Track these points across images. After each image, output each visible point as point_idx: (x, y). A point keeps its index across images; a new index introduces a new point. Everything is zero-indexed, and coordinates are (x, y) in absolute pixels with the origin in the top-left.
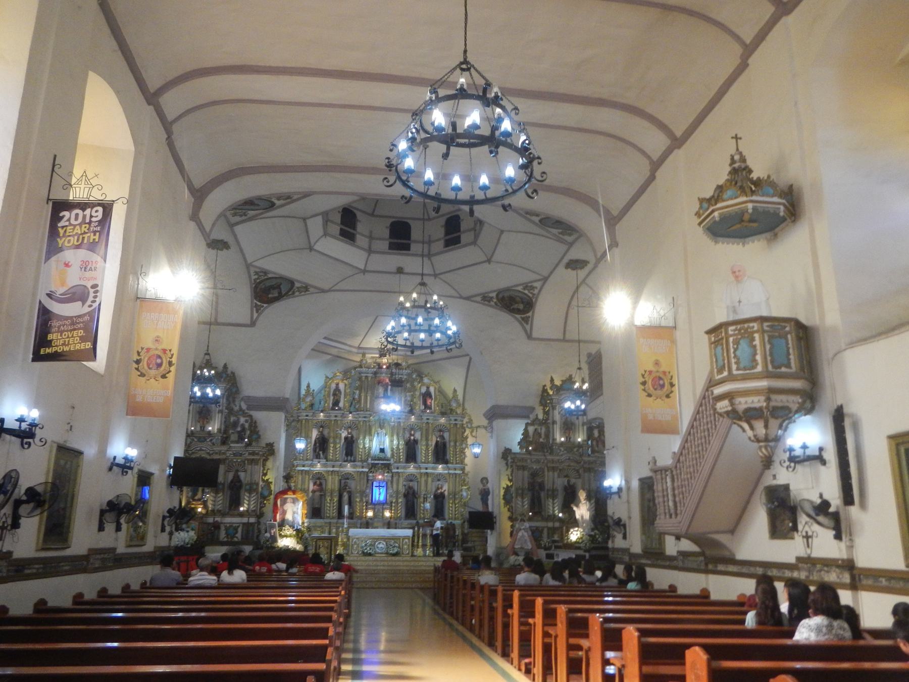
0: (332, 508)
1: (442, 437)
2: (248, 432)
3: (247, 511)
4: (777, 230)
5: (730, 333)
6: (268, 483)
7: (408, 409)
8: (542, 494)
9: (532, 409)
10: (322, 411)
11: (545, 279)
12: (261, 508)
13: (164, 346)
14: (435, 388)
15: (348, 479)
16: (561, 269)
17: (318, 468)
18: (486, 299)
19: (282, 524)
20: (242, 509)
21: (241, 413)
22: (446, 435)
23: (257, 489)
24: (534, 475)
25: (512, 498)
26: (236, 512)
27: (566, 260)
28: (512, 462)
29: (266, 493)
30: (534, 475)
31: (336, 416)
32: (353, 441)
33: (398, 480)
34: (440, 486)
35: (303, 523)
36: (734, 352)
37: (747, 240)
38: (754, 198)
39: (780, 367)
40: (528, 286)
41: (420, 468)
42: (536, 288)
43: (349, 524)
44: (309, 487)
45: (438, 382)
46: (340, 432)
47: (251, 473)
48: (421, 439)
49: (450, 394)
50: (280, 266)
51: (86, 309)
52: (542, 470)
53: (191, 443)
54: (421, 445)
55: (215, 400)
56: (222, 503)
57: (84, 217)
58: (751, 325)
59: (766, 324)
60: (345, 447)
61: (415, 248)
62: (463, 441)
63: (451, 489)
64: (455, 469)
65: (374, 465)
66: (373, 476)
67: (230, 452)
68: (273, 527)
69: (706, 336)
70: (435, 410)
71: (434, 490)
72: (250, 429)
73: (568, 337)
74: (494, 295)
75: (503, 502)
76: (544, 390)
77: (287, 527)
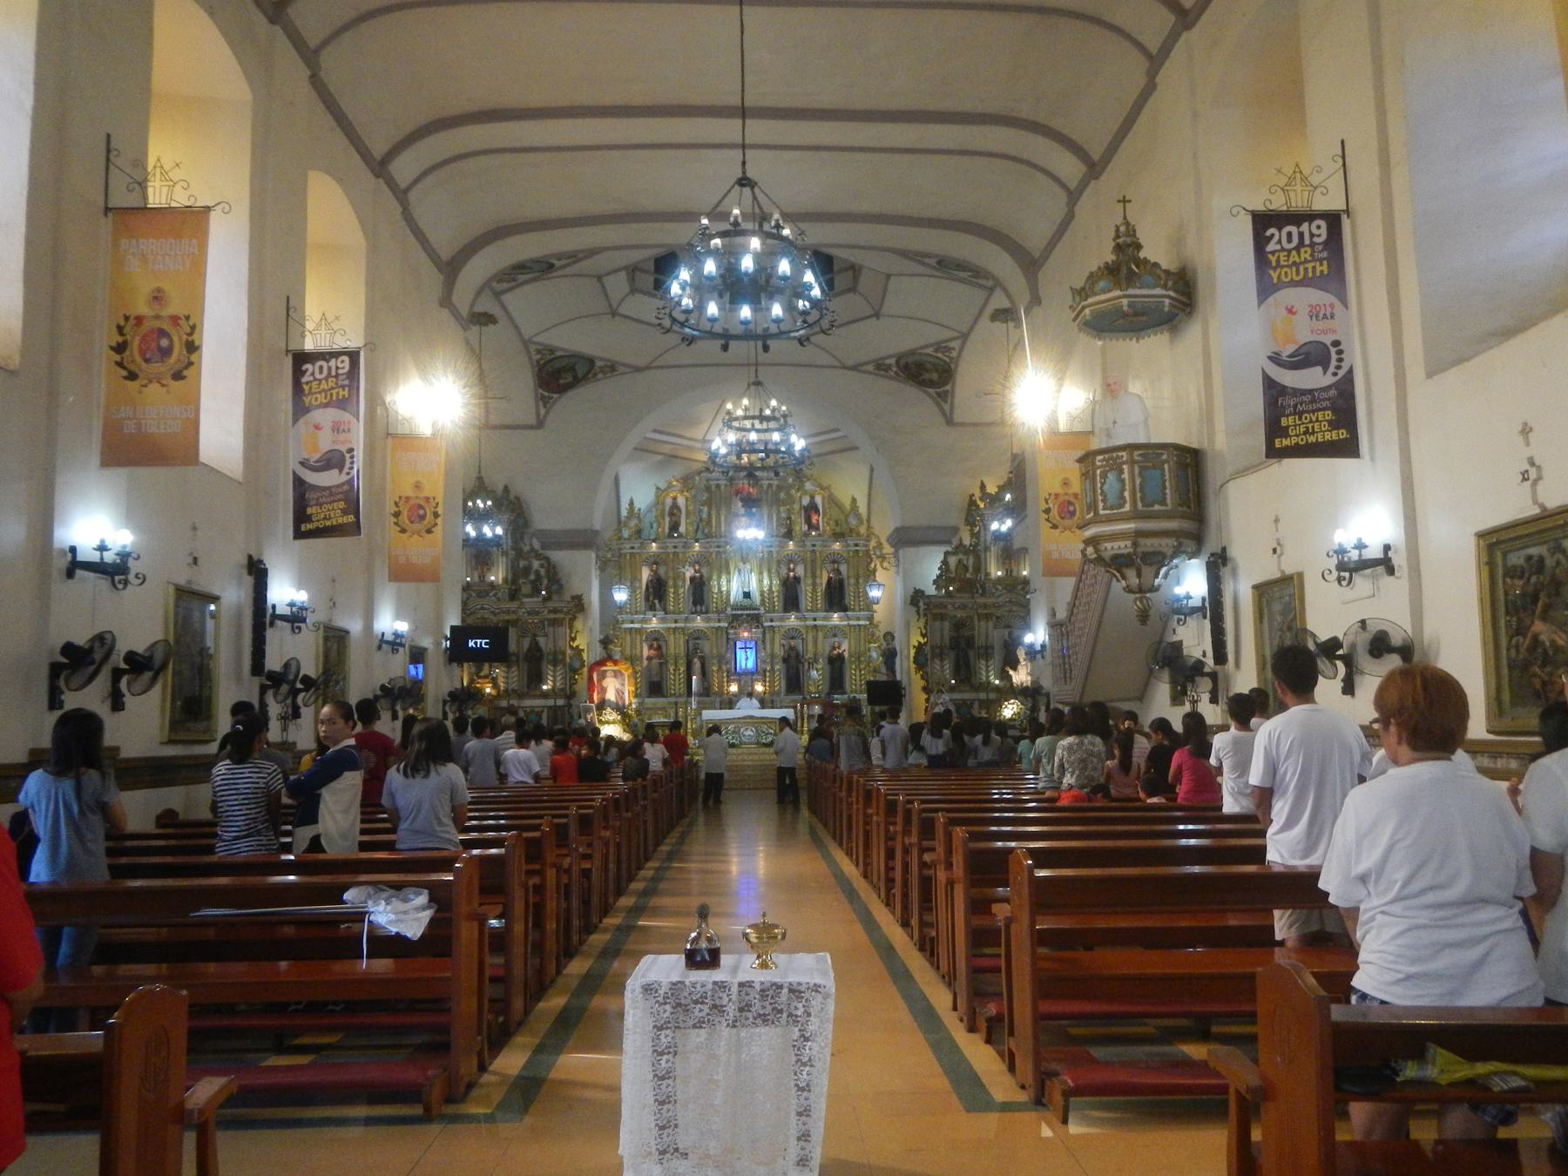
0: (677, 682)
1: (838, 572)
2: (545, 582)
3: (553, 689)
4: (1175, 322)
5: (1098, 463)
6: (578, 651)
7: (783, 530)
8: (971, 653)
9: (955, 530)
10: (654, 541)
11: (964, 337)
12: (571, 685)
13: (426, 493)
14: (823, 498)
15: (698, 638)
17: (654, 623)
18: (880, 367)
19: (602, 705)
20: (545, 687)
21: (533, 554)
22: (843, 568)
23: (564, 660)
24: (959, 625)
25: (927, 660)
26: (538, 693)
28: (925, 609)
29: (577, 665)
30: (959, 625)
31: (675, 547)
32: (704, 583)
33: (773, 639)
34: (836, 645)
35: (630, 704)
36: (1101, 488)
37: (1143, 333)
38: (1131, 291)
39: (1153, 506)
40: (940, 346)
41: (805, 619)
42: (953, 349)
43: (698, 703)
44: (642, 651)
45: (828, 488)
46: (683, 570)
47: (554, 638)
48: (805, 576)
49: (847, 504)
50: (571, 340)
51: (344, 478)
52: (971, 618)
53: (468, 599)
54: (806, 585)
55: (496, 541)
56: (518, 681)
57: (329, 368)
58: (1120, 454)
59: (1136, 453)
60: (691, 592)
62: (869, 576)
63: (853, 649)
64: (858, 619)
65: (735, 618)
66: (735, 633)
67: (524, 610)
68: (588, 710)
69: (1077, 465)
70: (824, 531)
71: (827, 651)
72: (548, 576)
74: (892, 361)
75: (913, 666)
76: (972, 503)
77: (609, 709)
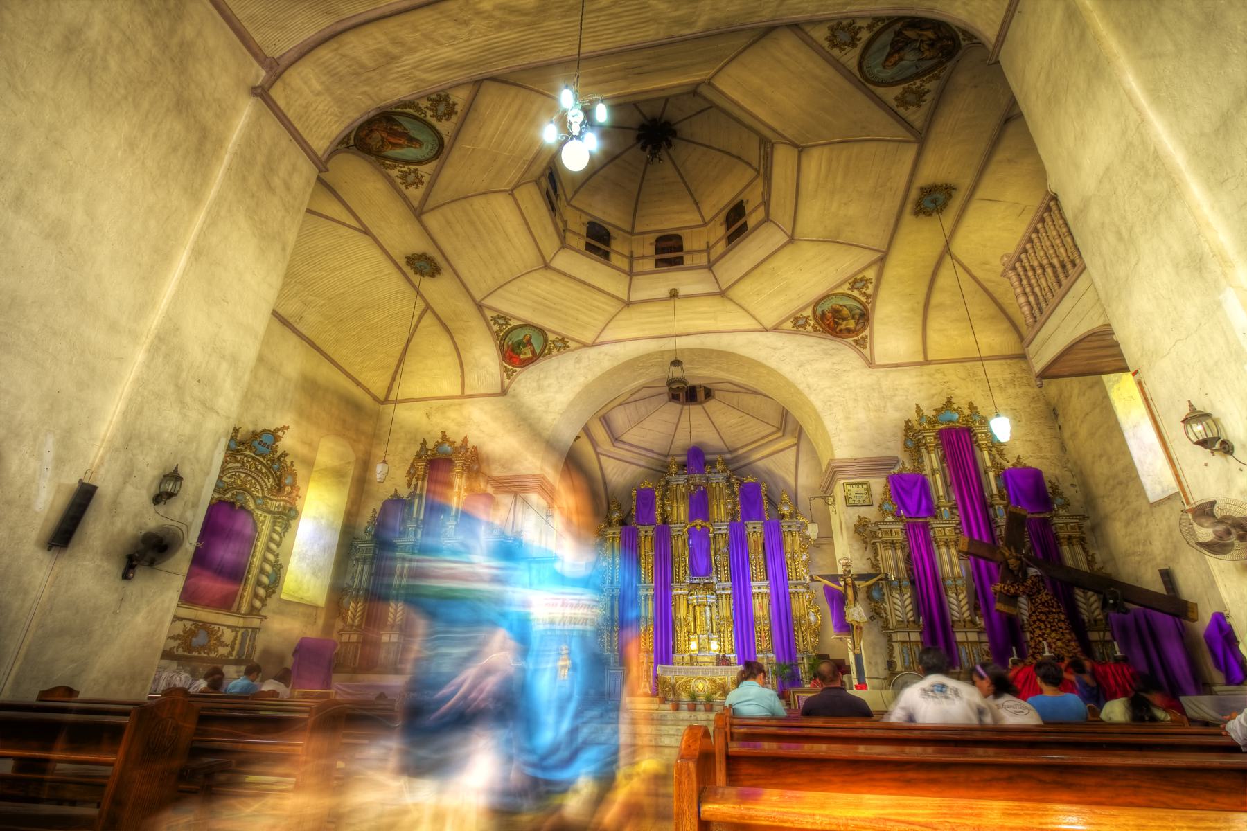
16: (908, 217)
27: (914, 194)
42: (868, 281)
61: (688, 261)
73: (930, 358)
74: (808, 312)
